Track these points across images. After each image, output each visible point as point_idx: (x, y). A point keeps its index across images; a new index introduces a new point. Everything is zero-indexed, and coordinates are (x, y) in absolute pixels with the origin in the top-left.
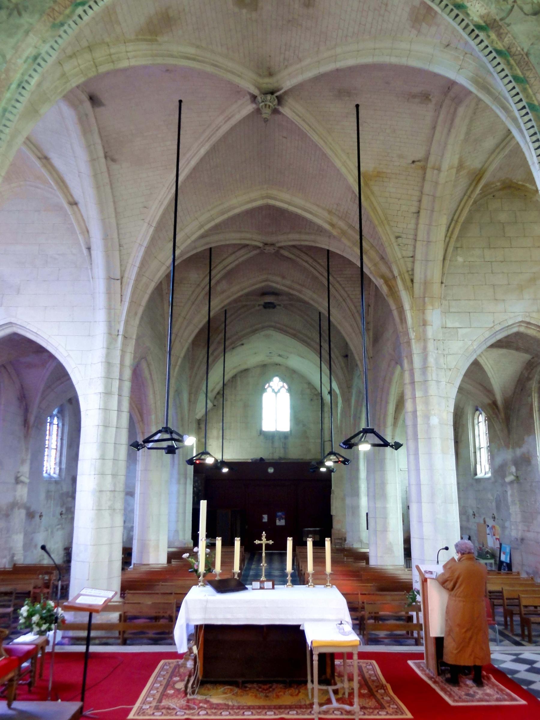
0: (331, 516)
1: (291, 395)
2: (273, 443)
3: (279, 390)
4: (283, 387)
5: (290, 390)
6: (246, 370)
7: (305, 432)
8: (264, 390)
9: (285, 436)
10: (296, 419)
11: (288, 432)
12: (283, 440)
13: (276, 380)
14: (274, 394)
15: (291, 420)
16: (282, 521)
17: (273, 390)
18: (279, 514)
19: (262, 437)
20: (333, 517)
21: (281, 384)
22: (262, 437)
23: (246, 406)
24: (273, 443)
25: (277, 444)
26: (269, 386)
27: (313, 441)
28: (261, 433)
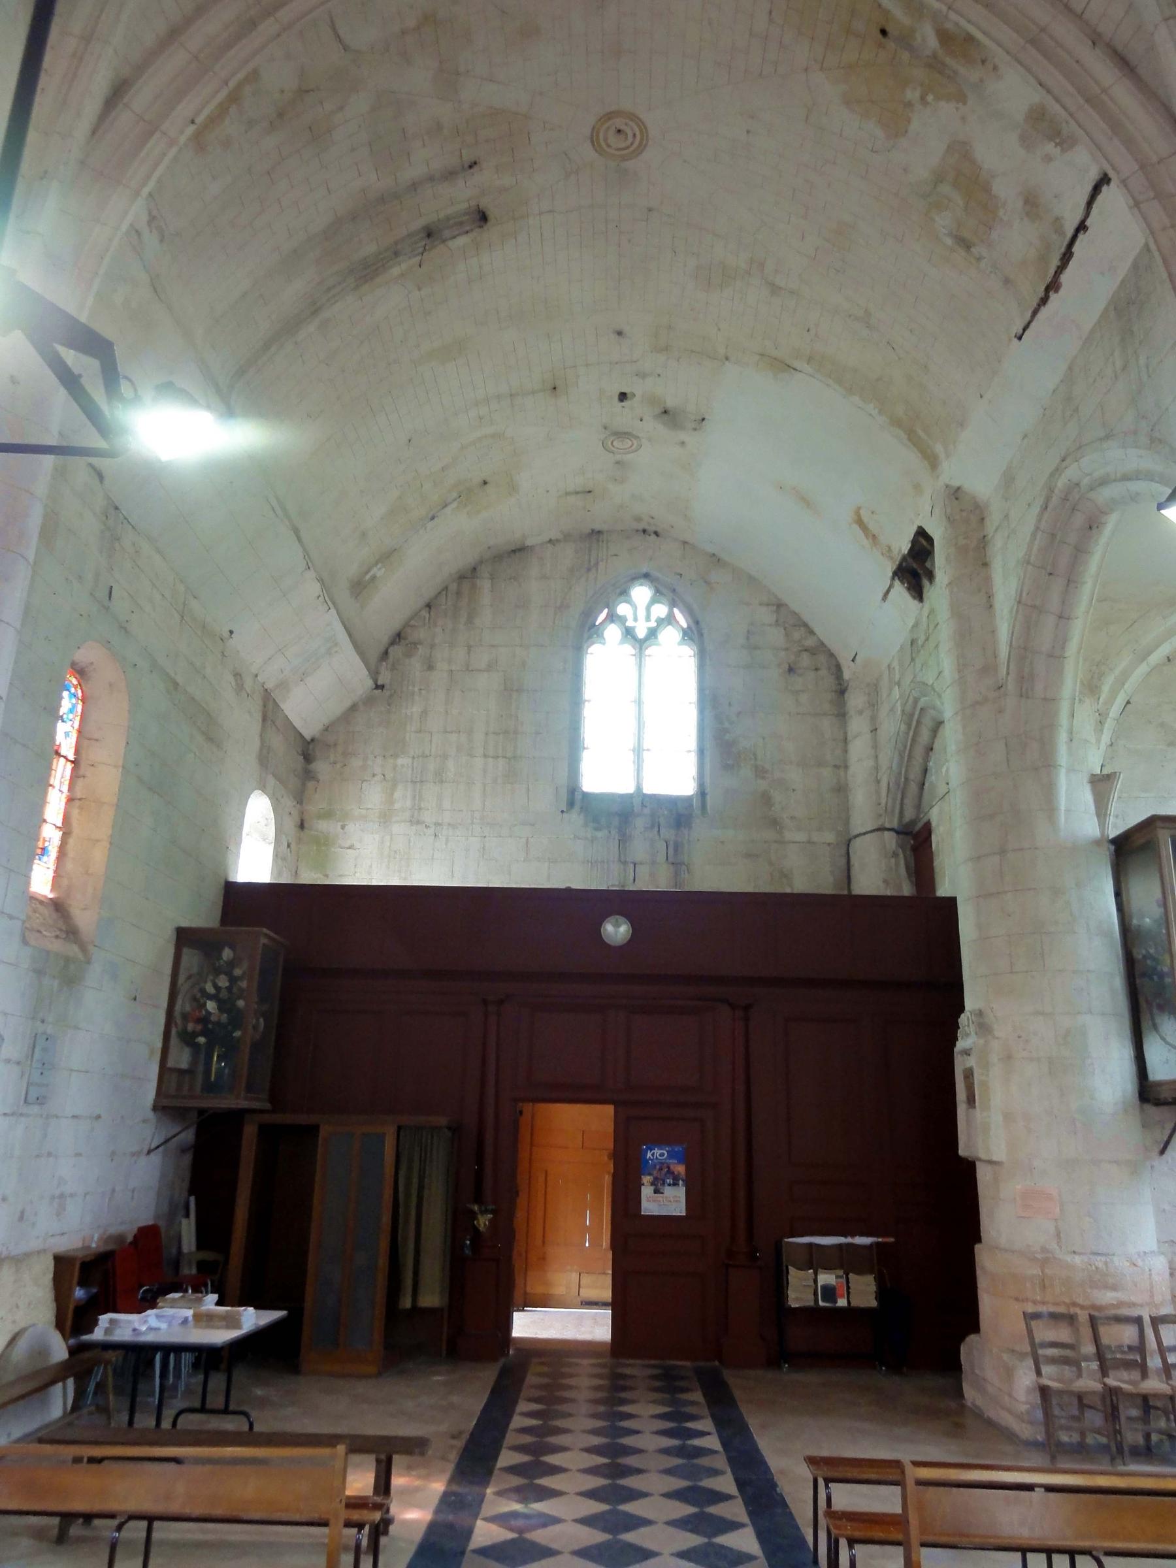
0: (967, 1171)
1: (703, 657)
2: (624, 840)
3: (652, 633)
4: (670, 620)
5: (695, 634)
6: (519, 551)
7: (766, 799)
8: (588, 631)
9: (676, 816)
10: (721, 741)
11: (689, 799)
12: (668, 833)
13: (641, 593)
14: (629, 649)
15: (701, 752)
16: (669, 1191)
17: (629, 633)
18: (656, 1154)
19: (575, 817)
20: (983, 1175)
21: (660, 610)
22: (575, 817)
23: (511, 690)
24: (624, 840)
25: (639, 849)
26: (612, 617)
27: (801, 837)
28: (575, 800)
